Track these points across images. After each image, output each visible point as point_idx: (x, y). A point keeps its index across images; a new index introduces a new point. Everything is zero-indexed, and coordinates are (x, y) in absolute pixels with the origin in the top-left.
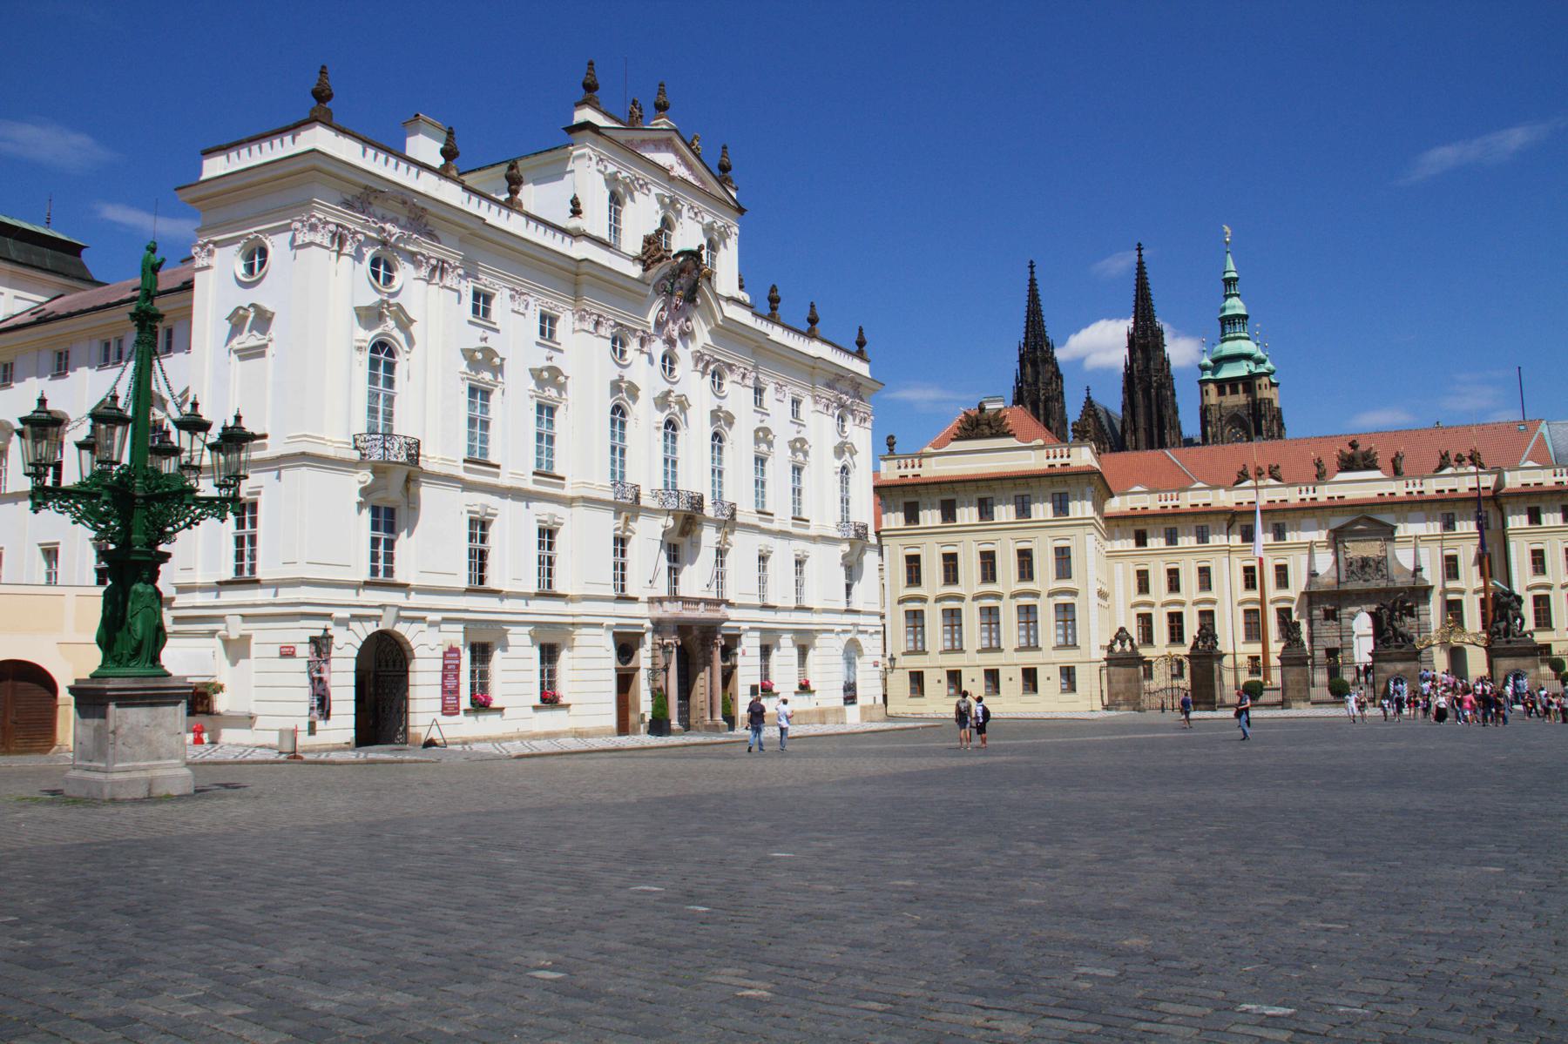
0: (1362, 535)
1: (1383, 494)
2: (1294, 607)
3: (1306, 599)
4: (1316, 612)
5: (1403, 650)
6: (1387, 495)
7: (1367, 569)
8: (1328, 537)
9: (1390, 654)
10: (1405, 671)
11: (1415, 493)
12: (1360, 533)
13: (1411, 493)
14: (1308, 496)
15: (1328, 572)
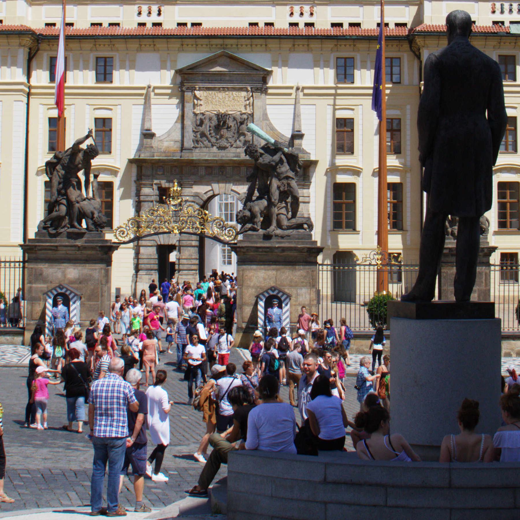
0: (221, 81)
1: (256, 24)
2: (117, 181)
3: (134, 170)
4: (146, 191)
5: (79, 243)
6: (261, 25)
7: (224, 131)
8: (173, 81)
9: (56, 248)
10: (81, 281)
11: (301, 26)
12: (219, 77)
13: (296, 24)
14: (149, 21)
15: (169, 133)
